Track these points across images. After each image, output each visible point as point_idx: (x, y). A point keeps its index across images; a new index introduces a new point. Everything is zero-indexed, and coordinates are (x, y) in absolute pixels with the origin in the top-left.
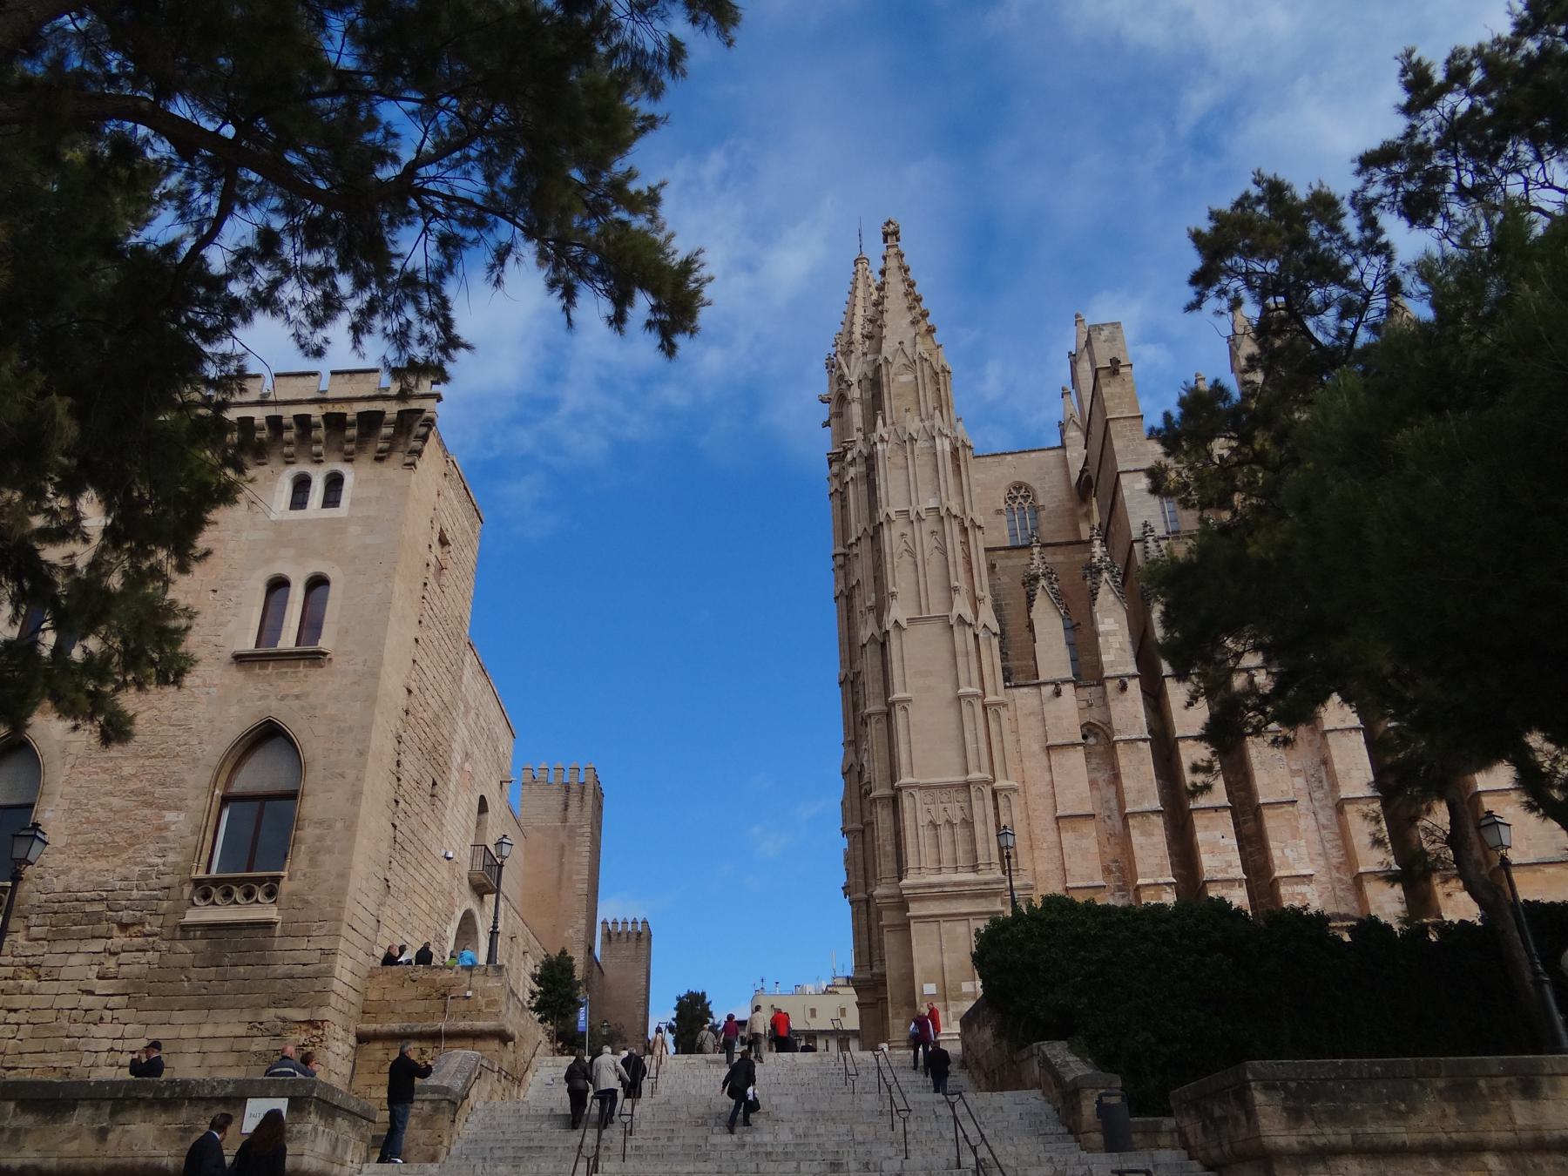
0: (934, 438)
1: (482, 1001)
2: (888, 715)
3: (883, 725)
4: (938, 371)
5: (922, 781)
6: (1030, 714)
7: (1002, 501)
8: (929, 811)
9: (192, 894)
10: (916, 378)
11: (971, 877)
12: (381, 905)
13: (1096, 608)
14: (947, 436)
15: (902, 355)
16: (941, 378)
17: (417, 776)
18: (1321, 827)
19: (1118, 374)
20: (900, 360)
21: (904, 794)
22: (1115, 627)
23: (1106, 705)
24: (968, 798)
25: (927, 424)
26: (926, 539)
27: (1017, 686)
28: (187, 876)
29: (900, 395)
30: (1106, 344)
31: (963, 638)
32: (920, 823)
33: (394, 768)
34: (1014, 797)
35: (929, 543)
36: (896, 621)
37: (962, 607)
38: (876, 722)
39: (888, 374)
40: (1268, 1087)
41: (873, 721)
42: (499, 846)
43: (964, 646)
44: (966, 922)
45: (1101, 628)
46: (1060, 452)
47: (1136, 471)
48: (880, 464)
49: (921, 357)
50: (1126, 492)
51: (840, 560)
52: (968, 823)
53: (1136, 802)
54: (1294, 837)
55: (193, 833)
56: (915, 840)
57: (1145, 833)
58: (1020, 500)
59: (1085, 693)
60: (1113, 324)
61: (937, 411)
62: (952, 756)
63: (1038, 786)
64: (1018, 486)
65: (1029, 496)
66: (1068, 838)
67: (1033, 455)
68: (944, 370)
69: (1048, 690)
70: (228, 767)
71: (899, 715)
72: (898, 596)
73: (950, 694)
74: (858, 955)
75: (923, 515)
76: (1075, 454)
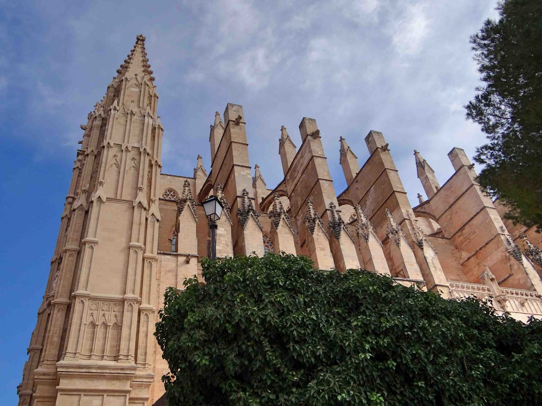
0: (144, 116)
3: (74, 258)
4: (153, 95)
5: (92, 294)
6: (169, 271)
7: (162, 195)
8: (92, 315)
10: (141, 91)
11: (113, 363)
15: (135, 80)
16: (153, 99)
19: (239, 125)
20: (134, 81)
21: (77, 301)
22: (225, 233)
24: (121, 310)
29: (129, 96)
30: (235, 112)
35: (130, 163)
36: (99, 197)
37: (142, 198)
38: (70, 256)
39: (126, 85)
46: (193, 180)
47: (242, 166)
48: (111, 120)
49: (145, 83)
50: (236, 174)
51: (70, 200)
52: (118, 327)
58: (170, 196)
60: (239, 106)
61: (149, 107)
65: (175, 196)
67: (180, 178)
69: (182, 259)
71: (87, 251)
72: (104, 184)
75: (130, 149)
76: (200, 182)
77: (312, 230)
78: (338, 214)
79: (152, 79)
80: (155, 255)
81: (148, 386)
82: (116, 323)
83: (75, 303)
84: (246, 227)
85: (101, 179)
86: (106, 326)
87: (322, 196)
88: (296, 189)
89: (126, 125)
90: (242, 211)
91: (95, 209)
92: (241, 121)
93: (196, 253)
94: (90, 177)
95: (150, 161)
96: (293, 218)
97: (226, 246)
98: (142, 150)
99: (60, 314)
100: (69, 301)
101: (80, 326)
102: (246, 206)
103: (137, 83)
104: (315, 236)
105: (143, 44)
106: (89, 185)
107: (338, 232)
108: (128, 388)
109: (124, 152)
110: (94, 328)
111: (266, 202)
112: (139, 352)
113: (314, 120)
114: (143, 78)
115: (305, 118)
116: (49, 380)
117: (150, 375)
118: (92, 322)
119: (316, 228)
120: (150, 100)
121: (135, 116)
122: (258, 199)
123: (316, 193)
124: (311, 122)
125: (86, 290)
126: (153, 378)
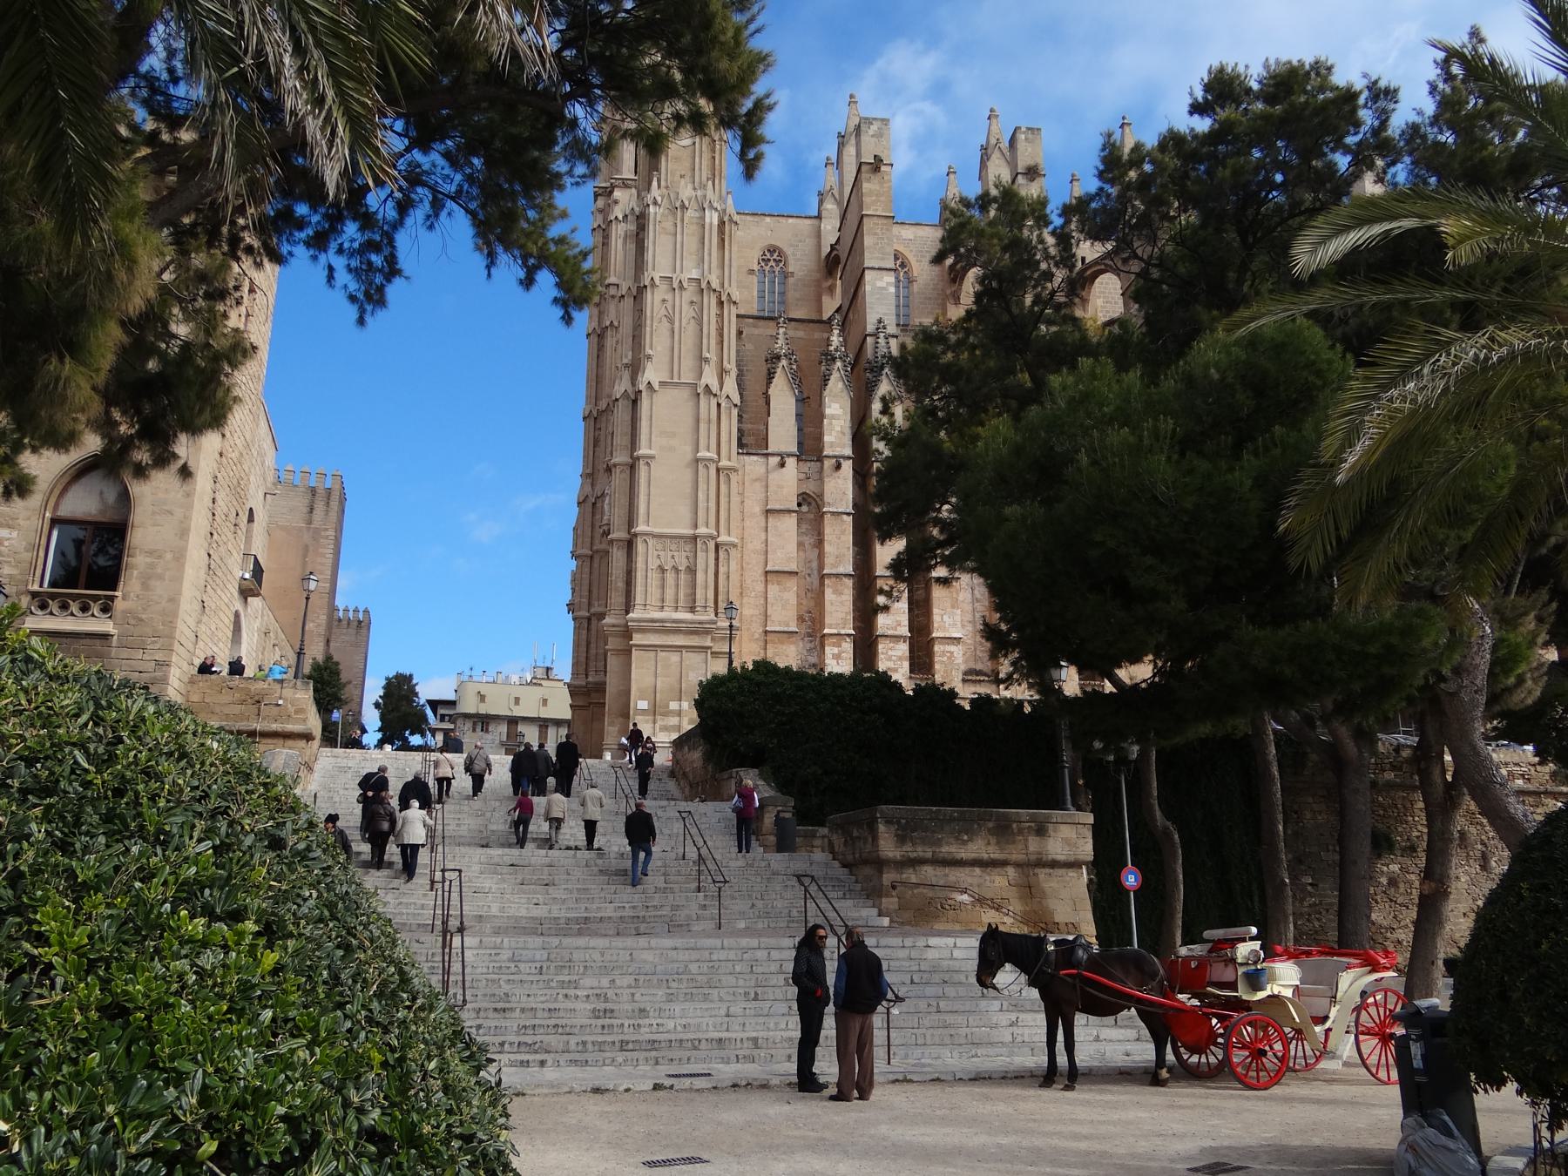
1: (291, 709)
2: (632, 467)
3: (626, 475)
5: (657, 530)
6: (756, 480)
7: (756, 261)
9: (30, 604)
11: (688, 616)
12: (199, 622)
13: (826, 393)
14: (716, 209)
17: (225, 509)
18: (975, 600)
22: (840, 412)
23: (821, 480)
25: (699, 193)
26: (685, 307)
27: (747, 454)
28: (23, 588)
31: (707, 407)
32: (650, 566)
33: (211, 505)
34: (733, 552)
35: (688, 312)
37: (710, 378)
40: (888, 822)
41: (618, 471)
42: (305, 582)
45: (828, 411)
47: (880, 269)
48: (651, 227)
50: (868, 288)
52: (692, 571)
53: (833, 566)
54: (953, 607)
55: (27, 550)
57: (837, 592)
58: (772, 263)
59: (806, 467)
60: (883, 120)
62: (685, 511)
63: (755, 544)
64: (772, 250)
66: (773, 590)
67: (791, 220)
69: (774, 460)
70: (57, 492)
73: (689, 456)
74: (575, 665)
76: (829, 227)
86: (676, 569)
99: (620, 553)
124: (1030, 136)
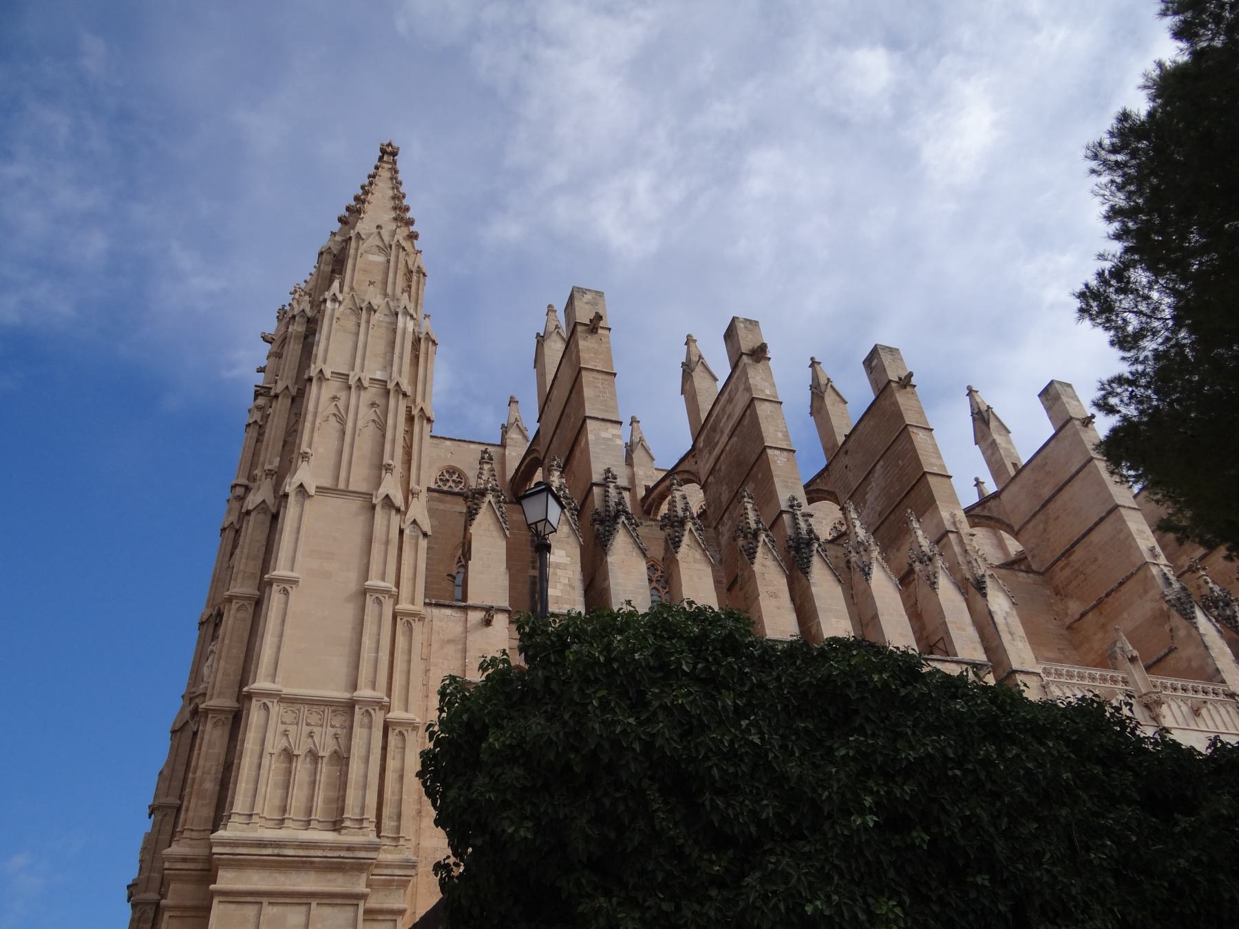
0: (397, 314)
2: (258, 604)
3: (247, 615)
4: (414, 269)
5: (287, 691)
7: (433, 480)
8: (285, 734)
10: (388, 261)
11: (329, 836)
15: (377, 238)
16: (415, 278)
19: (596, 333)
20: (374, 241)
21: (255, 703)
22: (566, 560)
24: (347, 724)
30: (587, 306)
32: (269, 747)
35: (366, 414)
36: (301, 485)
37: (391, 486)
38: (239, 609)
39: (357, 249)
43: (384, 529)
44: (303, 909)
46: (500, 450)
47: (603, 420)
49: (399, 245)
50: (591, 437)
51: (239, 491)
52: (341, 759)
56: (254, 773)
58: (451, 483)
60: (597, 292)
61: (406, 295)
62: (338, 664)
65: (461, 482)
67: (472, 446)
68: (419, 271)
69: (476, 617)
71: (275, 599)
72: (312, 459)
73: (353, 586)
75: (366, 384)
76: (514, 454)
77: (752, 555)
78: (807, 521)
79: (413, 236)
80: (418, 607)
81: (403, 884)
82: (336, 752)
83: (249, 710)
84: (612, 548)
85: (304, 448)
86: (314, 756)
87: (773, 483)
88: (717, 467)
89: (358, 334)
90: (603, 514)
91: (291, 510)
92: (602, 324)
93: (505, 604)
94: (281, 443)
95: (409, 409)
96: (711, 530)
97: (568, 589)
98: (391, 386)
99: (217, 733)
100: (236, 705)
101: (261, 757)
102: (612, 504)
103: (381, 244)
104: (757, 567)
105: (395, 162)
106: (278, 459)
107: (807, 558)
108: (361, 888)
109: (353, 389)
110: (290, 762)
111: (653, 496)
112: (386, 811)
113: (756, 322)
114: (394, 233)
115: (737, 318)
116: (193, 873)
117: (408, 861)
118: (285, 750)
119: (760, 550)
120: (409, 280)
121: (377, 314)
122: (638, 490)
123: (760, 476)
124: (749, 326)
125: (274, 682)
126: (414, 867)
